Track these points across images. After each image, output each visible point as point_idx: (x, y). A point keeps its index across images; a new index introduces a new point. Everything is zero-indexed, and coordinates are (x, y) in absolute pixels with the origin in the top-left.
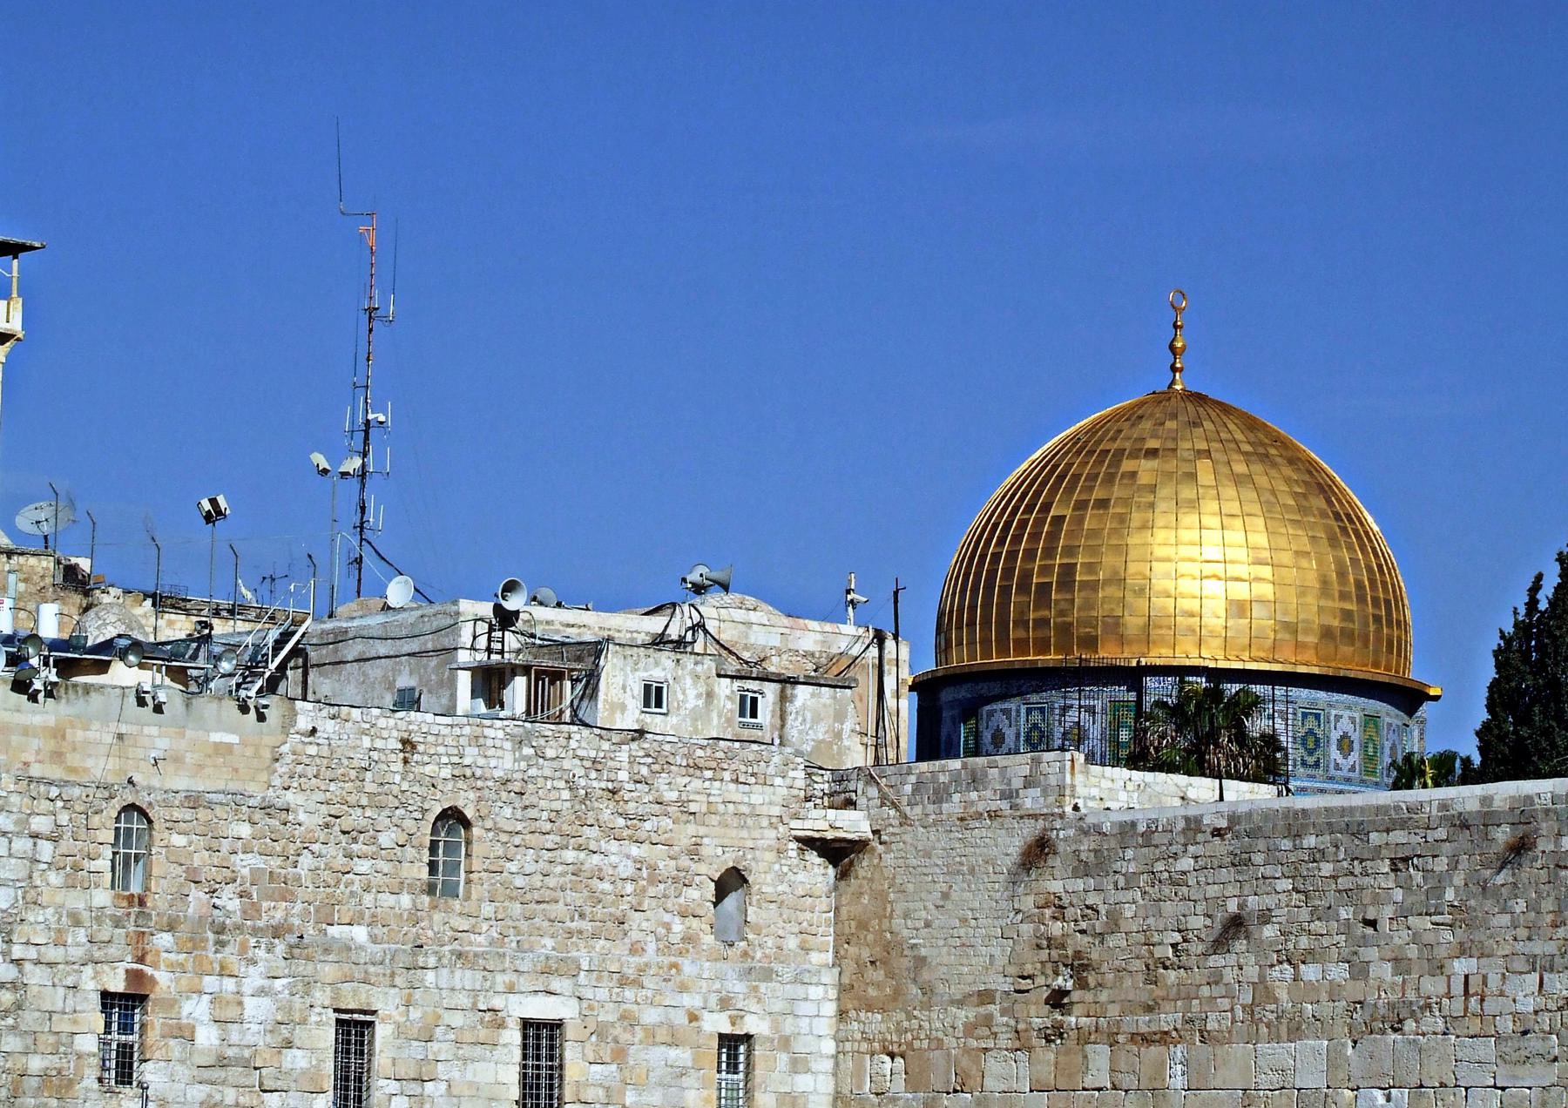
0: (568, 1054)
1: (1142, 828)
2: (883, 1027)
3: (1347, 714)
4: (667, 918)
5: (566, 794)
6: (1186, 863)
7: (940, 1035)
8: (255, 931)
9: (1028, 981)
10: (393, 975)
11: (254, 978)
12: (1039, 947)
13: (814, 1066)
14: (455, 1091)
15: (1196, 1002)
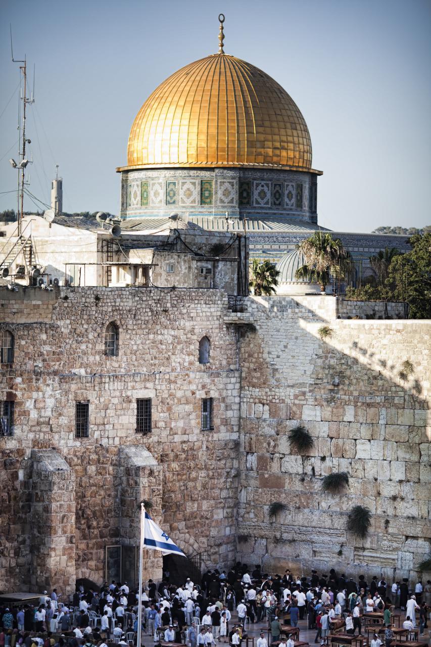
0: (152, 411)
1: (367, 327)
2: (260, 394)
3: (290, 184)
4: (184, 356)
5: (150, 314)
6: (385, 341)
7: (284, 398)
8: (49, 374)
9: (320, 381)
10: (94, 386)
11: (49, 391)
12: (324, 368)
13: (233, 407)
14: (115, 427)
15: (389, 392)
